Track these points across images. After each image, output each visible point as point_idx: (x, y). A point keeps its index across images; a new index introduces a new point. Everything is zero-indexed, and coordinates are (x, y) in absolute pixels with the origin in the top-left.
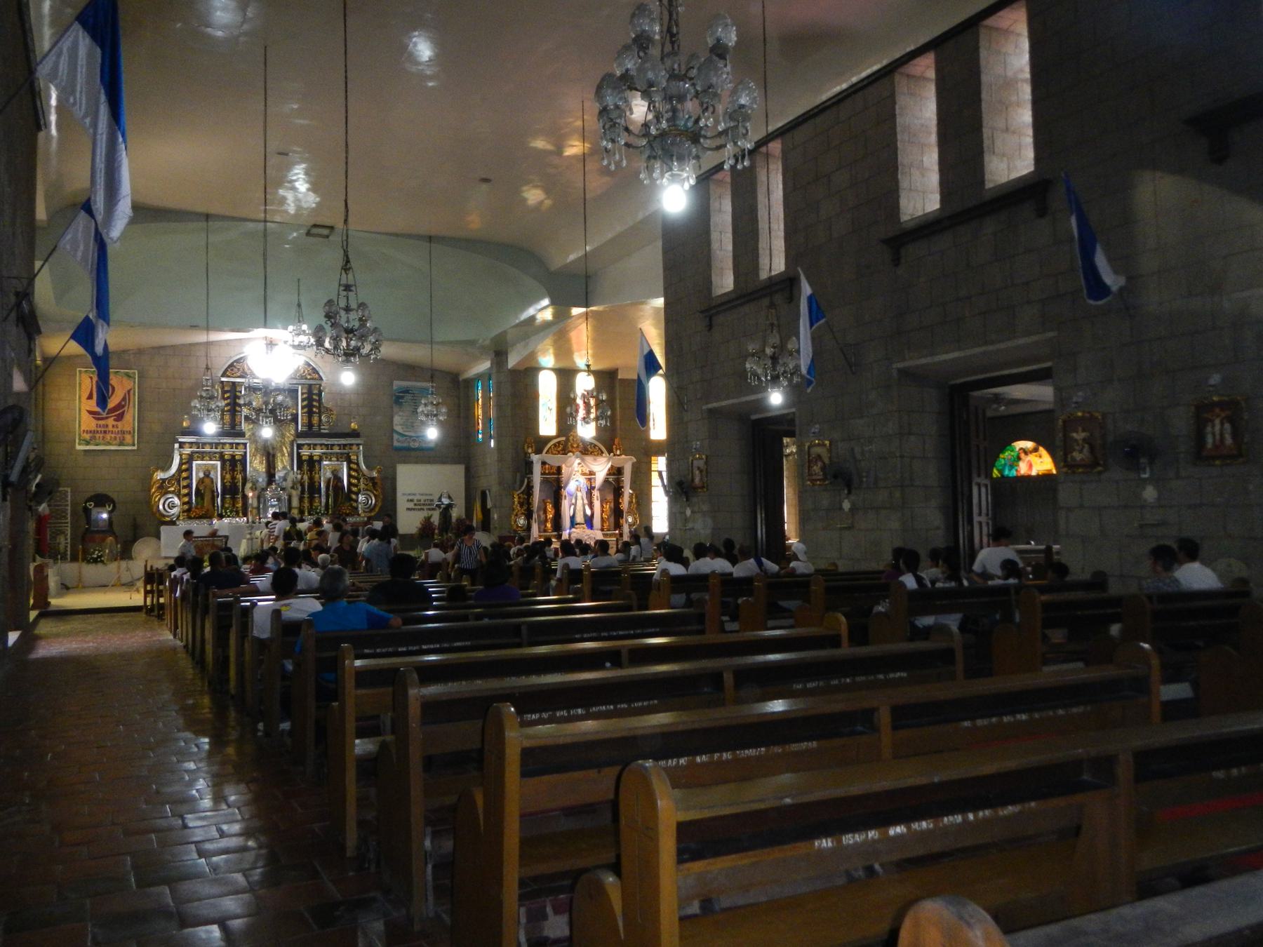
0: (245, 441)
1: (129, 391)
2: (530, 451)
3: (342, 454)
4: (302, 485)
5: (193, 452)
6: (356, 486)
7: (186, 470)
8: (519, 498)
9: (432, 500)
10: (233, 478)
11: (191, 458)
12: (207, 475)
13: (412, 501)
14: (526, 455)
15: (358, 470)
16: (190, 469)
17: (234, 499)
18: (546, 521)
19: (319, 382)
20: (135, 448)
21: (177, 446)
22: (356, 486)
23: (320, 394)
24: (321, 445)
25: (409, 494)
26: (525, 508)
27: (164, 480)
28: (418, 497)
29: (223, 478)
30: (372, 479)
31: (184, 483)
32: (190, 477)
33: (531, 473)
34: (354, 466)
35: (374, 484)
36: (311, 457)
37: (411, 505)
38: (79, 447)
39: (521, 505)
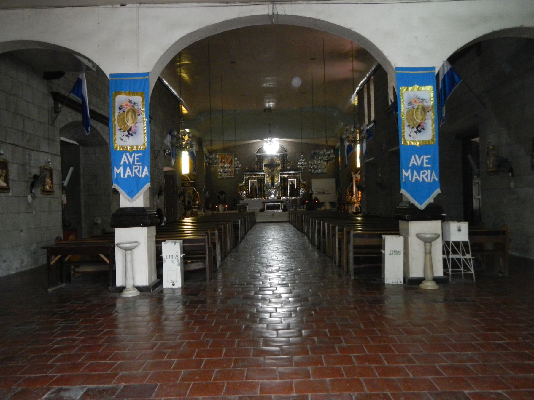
0: (264, 173)
1: (231, 159)
2: (353, 173)
3: (294, 176)
4: (281, 186)
5: (249, 178)
6: (299, 187)
7: (247, 183)
8: (349, 190)
9: (324, 191)
10: (261, 185)
11: (249, 179)
12: (253, 184)
13: (317, 191)
14: (351, 174)
15: (300, 181)
16: (248, 183)
17: (261, 192)
18: (359, 198)
19: (286, 153)
20: (234, 177)
21: (244, 176)
22: (299, 187)
23: (287, 156)
24: (287, 173)
25: (316, 189)
26: (351, 193)
27: (241, 186)
28: (319, 190)
29: (258, 185)
30: (304, 184)
31: (247, 187)
32: (248, 185)
33: (353, 181)
34: (298, 180)
35: (305, 186)
36: (284, 177)
37: (317, 193)
38: (219, 177)
39: (350, 192)
